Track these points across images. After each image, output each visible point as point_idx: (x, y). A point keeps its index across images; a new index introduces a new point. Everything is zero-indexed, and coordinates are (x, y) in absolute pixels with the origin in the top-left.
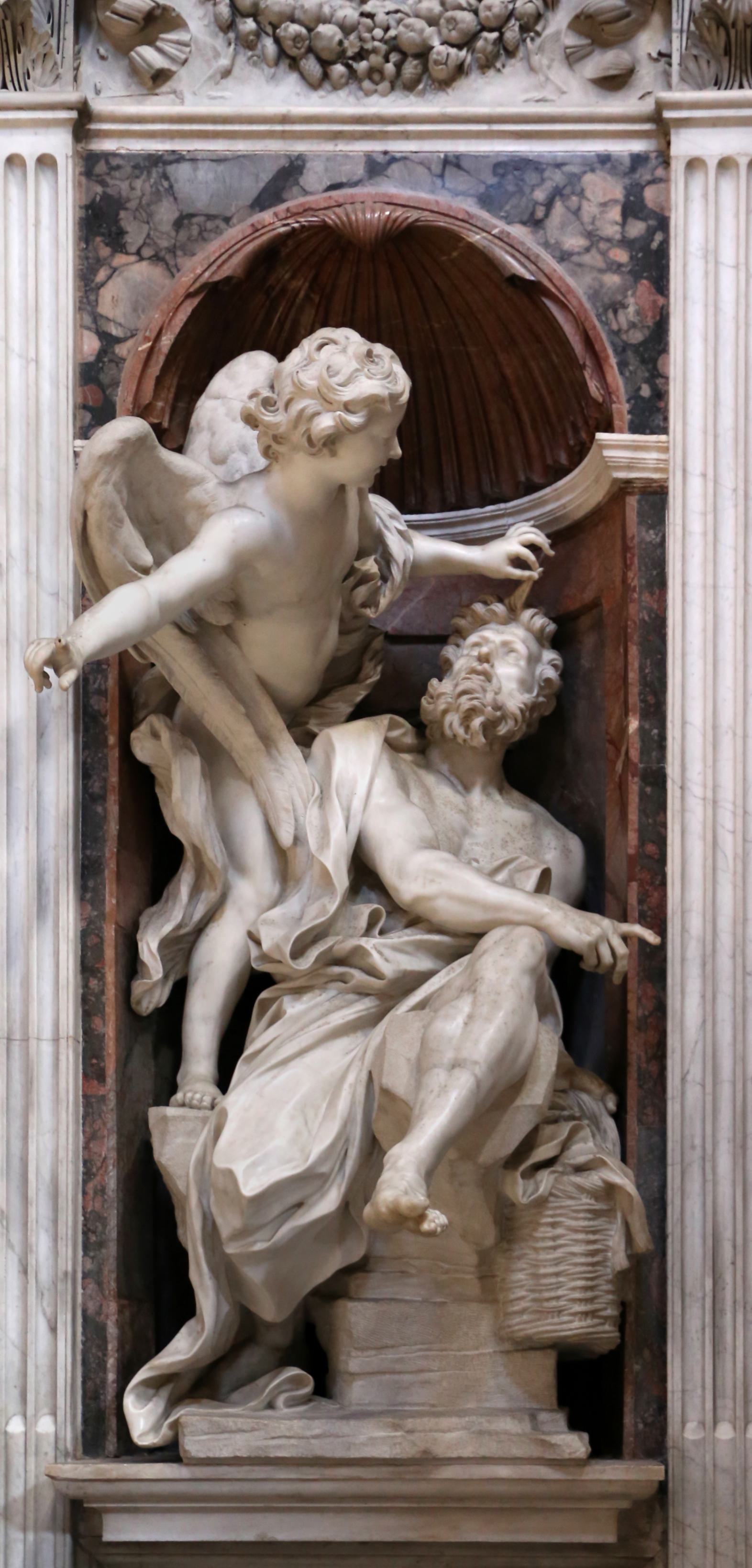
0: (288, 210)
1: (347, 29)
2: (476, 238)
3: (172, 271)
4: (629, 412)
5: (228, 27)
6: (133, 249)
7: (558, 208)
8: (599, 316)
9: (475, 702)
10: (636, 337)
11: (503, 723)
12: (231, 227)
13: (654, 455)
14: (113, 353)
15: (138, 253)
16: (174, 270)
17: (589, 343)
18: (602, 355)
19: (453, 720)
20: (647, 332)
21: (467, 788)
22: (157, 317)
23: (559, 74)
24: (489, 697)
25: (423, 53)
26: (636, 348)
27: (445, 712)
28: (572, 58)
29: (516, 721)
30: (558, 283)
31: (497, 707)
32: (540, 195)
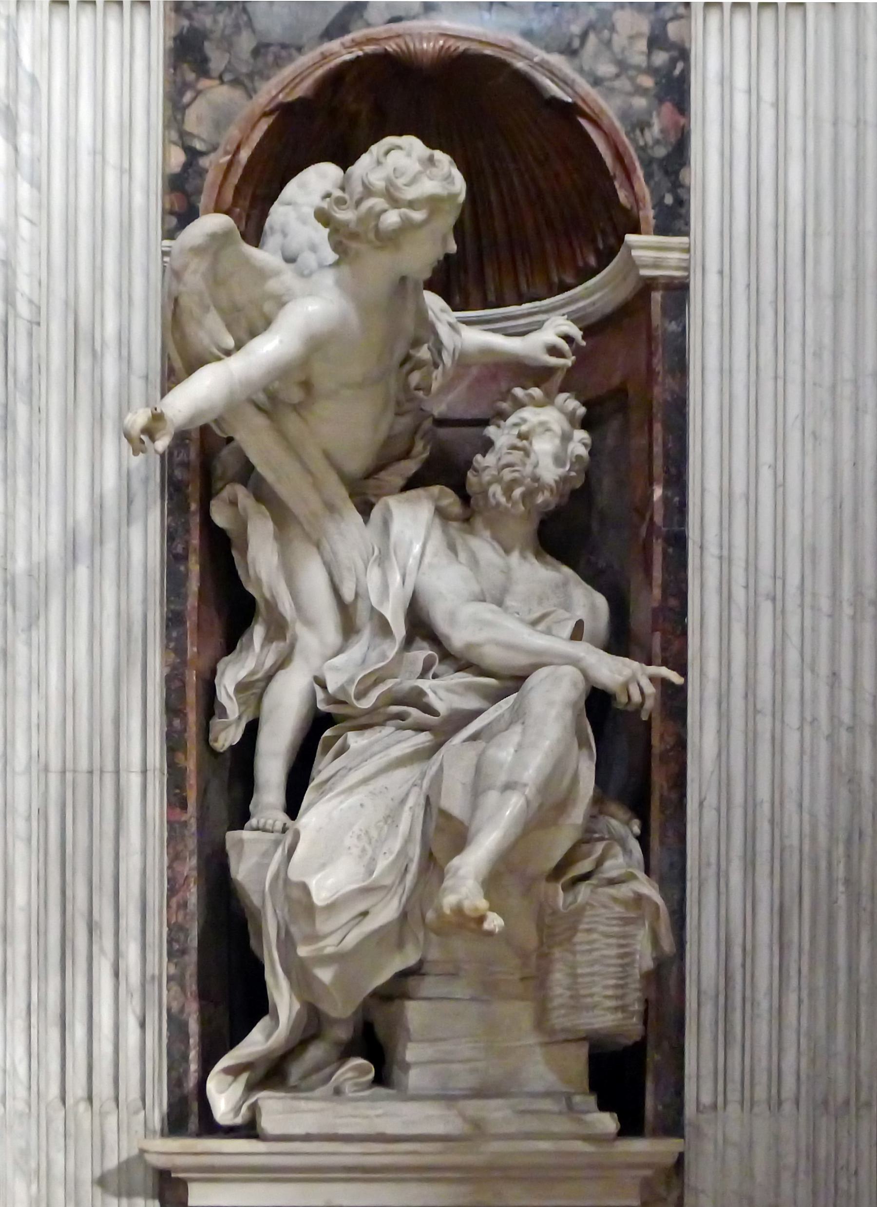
0: (353, 40)
3: (250, 93)
6: (215, 74)
7: (592, 39)
8: (627, 134)
9: (516, 475)
10: (661, 152)
11: (540, 494)
12: (303, 55)
15: (220, 78)
17: (619, 156)
19: (496, 490)
20: (670, 149)
21: (507, 551)
24: (528, 469)
26: (661, 161)
29: (552, 491)
30: (592, 105)
31: (536, 479)
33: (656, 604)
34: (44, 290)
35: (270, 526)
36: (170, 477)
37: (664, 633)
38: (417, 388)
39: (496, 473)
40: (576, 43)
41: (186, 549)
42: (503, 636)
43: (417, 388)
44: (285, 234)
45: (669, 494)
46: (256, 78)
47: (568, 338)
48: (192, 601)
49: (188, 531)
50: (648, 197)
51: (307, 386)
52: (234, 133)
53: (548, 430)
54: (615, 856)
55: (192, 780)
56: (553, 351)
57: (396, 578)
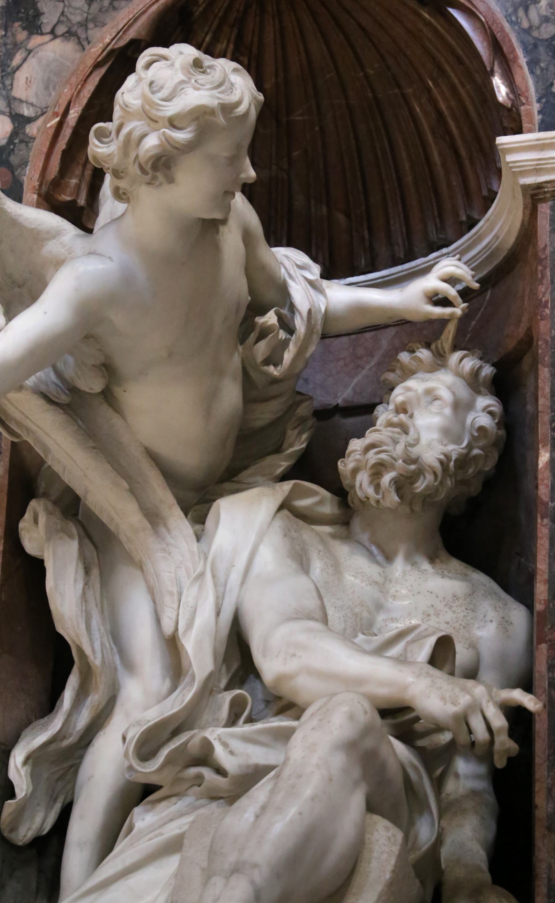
9: (383, 456)
14: (24, 133)
16: (85, 43)
18: (511, 56)
21: (389, 558)
22: (67, 92)
27: (355, 471)
29: (435, 473)
38: (267, 362)
42: (317, 663)
43: (267, 362)
47: (451, 280)
53: (436, 398)
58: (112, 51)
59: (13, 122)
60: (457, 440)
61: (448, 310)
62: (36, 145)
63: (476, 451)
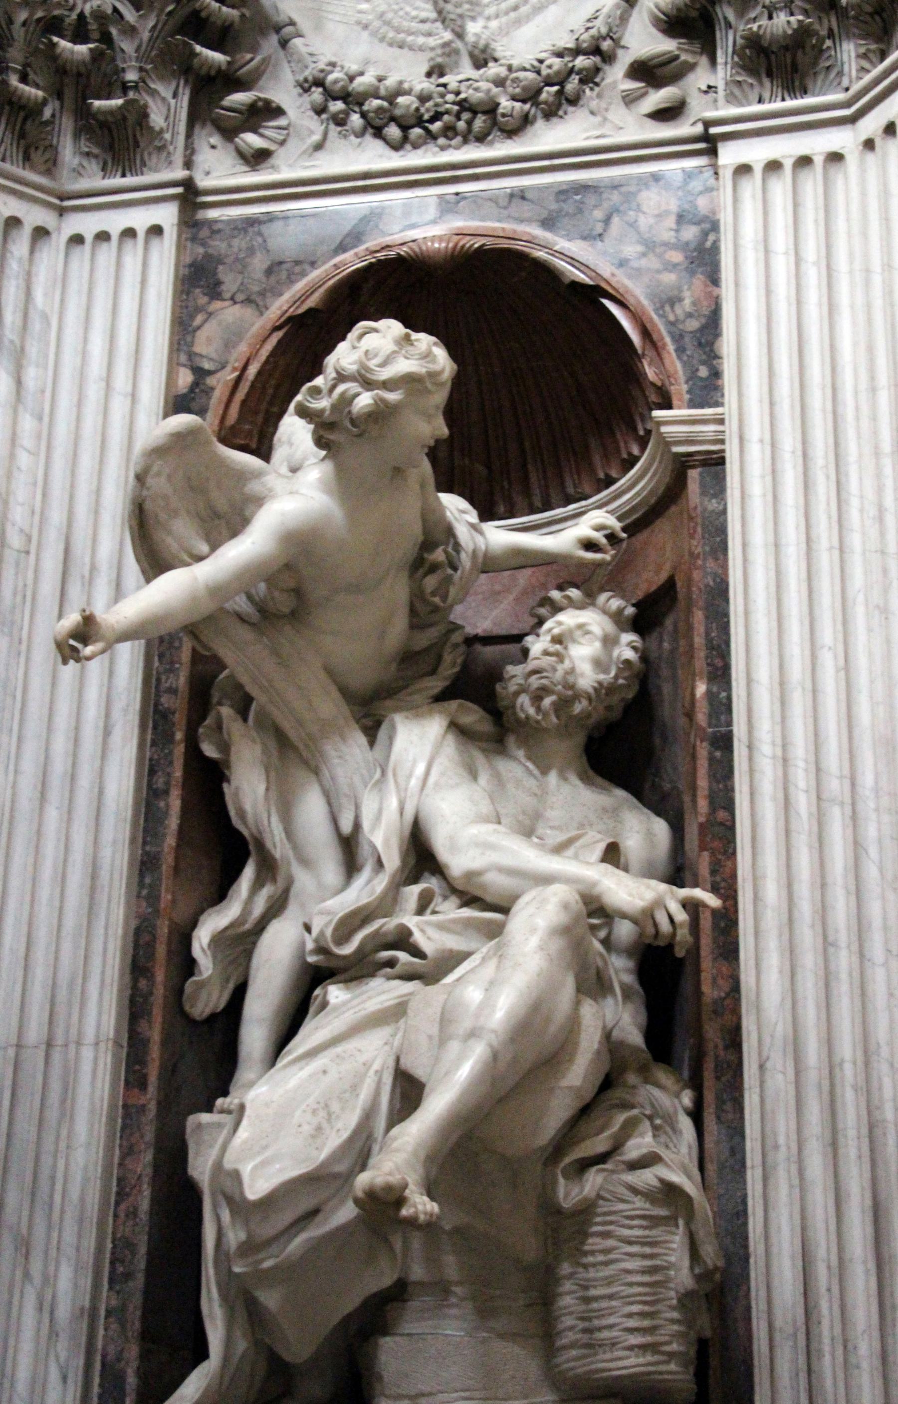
0: (367, 249)
1: (424, 98)
2: (541, 254)
4: (688, 392)
5: (320, 111)
6: (227, 295)
7: (616, 220)
8: (656, 310)
9: (544, 681)
10: (693, 325)
13: (712, 427)
15: (232, 298)
17: (646, 333)
18: (659, 344)
19: (524, 700)
23: (618, 114)
24: (559, 675)
25: (491, 109)
27: (517, 694)
28: (630, 100)
29: (590, 699)
32: (598, 214)
33: (702, 819)
34: (37, 518)
35: (258, 749)
36: (156, 705)
37: (713, 854)
38: (433, 594)
39: (522, 682)
40: (599, 228)
41: (168, 783)
43: (433, 594)
44: (291, 444)
45: (715, 689)
46: (269, 294)
48: (170, 841)
49: (171, 763)
50: (680, 372)
51: (298, 592)
52: (243, 349)
54: (642, 1135)
55: (155, 1052)
56: (589, 545)
57: (393, 803)
58: (290, 319)
59: (194, 374)
60: (606, 671)
61: (598, 556)
62: (217, 394)
63: (621, 681)
